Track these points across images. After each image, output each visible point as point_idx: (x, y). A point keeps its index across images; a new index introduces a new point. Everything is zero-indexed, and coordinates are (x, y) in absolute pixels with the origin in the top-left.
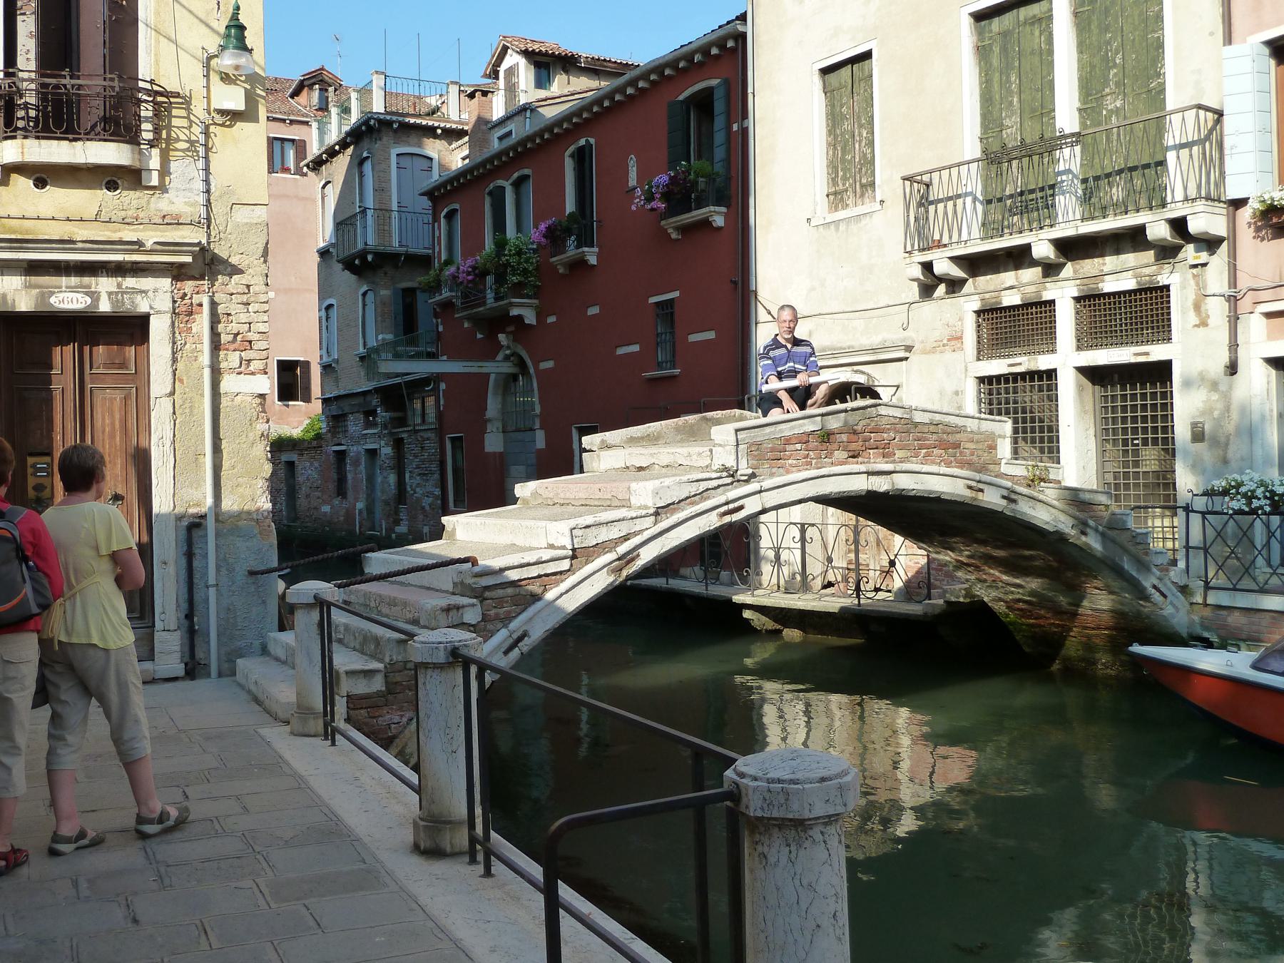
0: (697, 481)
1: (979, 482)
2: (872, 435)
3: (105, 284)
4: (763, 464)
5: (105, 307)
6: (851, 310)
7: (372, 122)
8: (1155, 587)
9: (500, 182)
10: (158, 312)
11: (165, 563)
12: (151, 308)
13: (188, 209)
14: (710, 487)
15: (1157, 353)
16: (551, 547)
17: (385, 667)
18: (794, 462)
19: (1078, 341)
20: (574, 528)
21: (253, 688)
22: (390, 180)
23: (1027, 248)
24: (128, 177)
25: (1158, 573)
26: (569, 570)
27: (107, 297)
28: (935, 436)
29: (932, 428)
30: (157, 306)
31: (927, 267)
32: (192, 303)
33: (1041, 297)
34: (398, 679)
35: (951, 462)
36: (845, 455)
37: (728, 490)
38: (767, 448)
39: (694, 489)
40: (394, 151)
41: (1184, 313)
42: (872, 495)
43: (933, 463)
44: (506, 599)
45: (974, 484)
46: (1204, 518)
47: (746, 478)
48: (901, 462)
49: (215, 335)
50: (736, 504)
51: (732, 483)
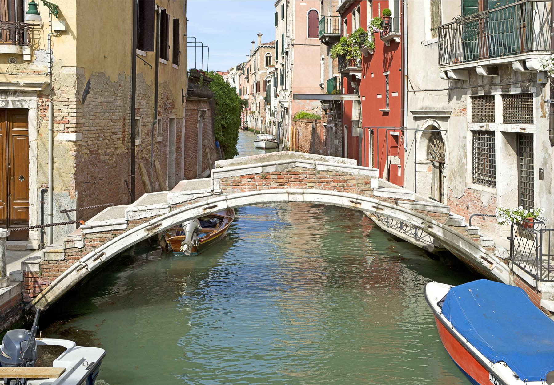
0: (192, 194)
1: (357, 199)
3: (10, 99)
4: (229, 187)
5: (11, 106)
6: (434, 89)
8: (483, 258)
10: (32, 109)
11: (33, 205)
12: (29, 107)
13: (44, 69)
14: (199, 197)
15: (529, 129)
18: (246, 187)
19: (504, 117)
20: (129, 212)
23: (474, 69)
24: (16, 58)
25: (484, 251)
26: (126, 229)
27: (11, 103)
28: (331, 177)
29: (329, 173)
30: (31, 106)
32: (46, 105)
34: (45, 267)
35: (341, 189)
36: (277, 184)
37: (210, 199)
38: (231, 181)
39: (190, 197)
41: (537, 109)
43: (329, 189)
47: (219, 193)
48: (309, 188)
49: (53, 118)
50: (213, 205)
51: (212, 195)
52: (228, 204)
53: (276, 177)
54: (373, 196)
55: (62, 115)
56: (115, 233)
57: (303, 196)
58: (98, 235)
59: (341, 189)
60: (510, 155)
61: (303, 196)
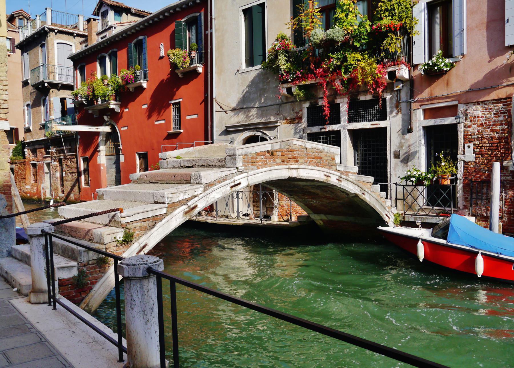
1: (329, 173)
2: (290, 152)
7: (46, 29)
9: (104, 54)
15: (382, 124)
16: (157, 203)
17: (78, 264)
21: (5, 275)
22: (54, 53)
26: (166, 214)
28: (313, 154)
31: (289, 90)
33: (334, 102)
40: (56, 42)
41: (391, 107)
42: (291, 179)
43: (313, 165)
44: (137, 228)
45: (327, 174)
46: (404, 188)
54: (337, 170)
56: (155, 220)
57: (297, 172)
58: (139, 224)
61: (297, 172)
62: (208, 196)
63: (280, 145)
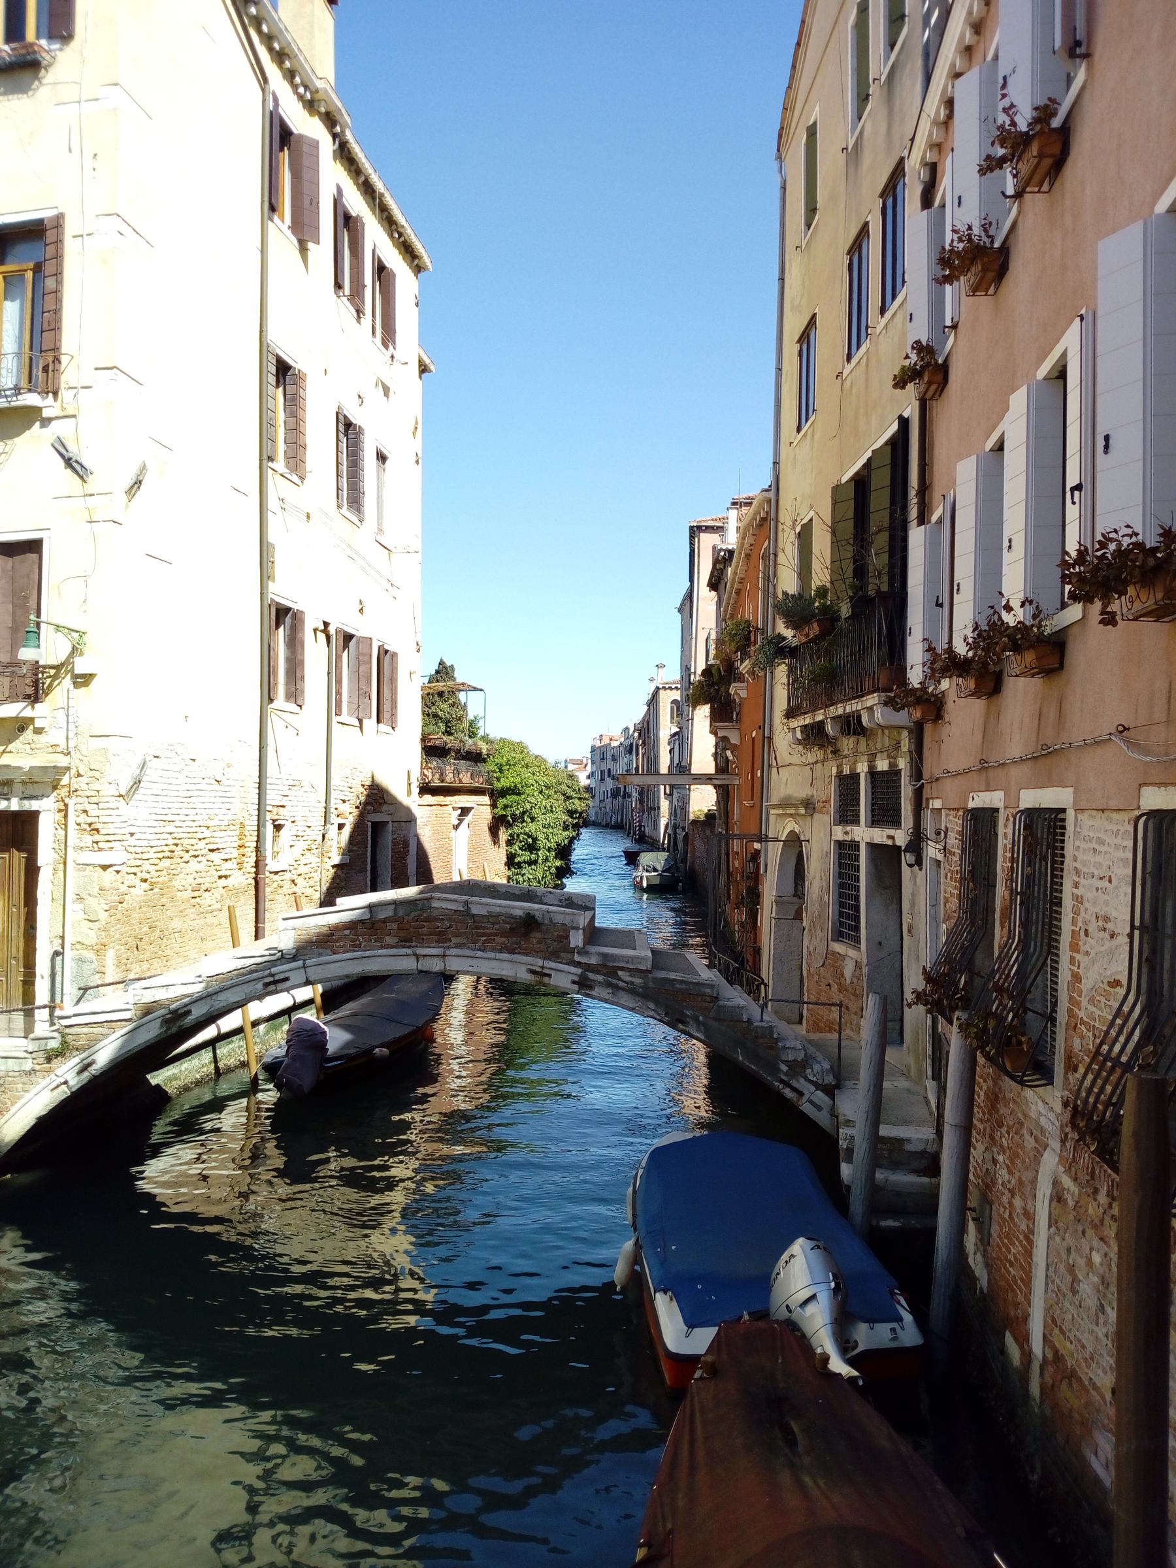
35: (515, 949)
36: (396, 940)
48: (456, 947)
50: (282, 976)
52: (309, 975)
53: (395, 926)
55: (89, 820)
59: (515, 949)
60: (885, 888)
62: (214, 997)
63: (395, 910)
